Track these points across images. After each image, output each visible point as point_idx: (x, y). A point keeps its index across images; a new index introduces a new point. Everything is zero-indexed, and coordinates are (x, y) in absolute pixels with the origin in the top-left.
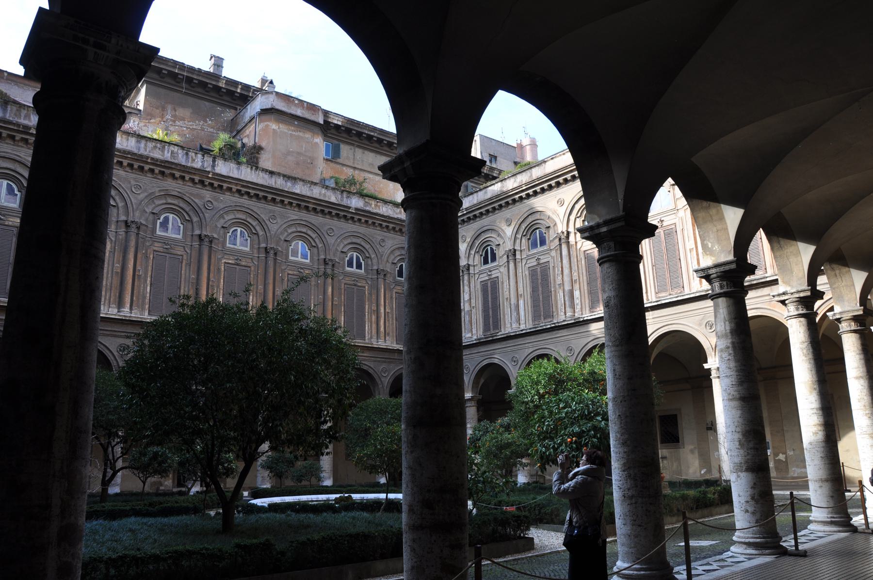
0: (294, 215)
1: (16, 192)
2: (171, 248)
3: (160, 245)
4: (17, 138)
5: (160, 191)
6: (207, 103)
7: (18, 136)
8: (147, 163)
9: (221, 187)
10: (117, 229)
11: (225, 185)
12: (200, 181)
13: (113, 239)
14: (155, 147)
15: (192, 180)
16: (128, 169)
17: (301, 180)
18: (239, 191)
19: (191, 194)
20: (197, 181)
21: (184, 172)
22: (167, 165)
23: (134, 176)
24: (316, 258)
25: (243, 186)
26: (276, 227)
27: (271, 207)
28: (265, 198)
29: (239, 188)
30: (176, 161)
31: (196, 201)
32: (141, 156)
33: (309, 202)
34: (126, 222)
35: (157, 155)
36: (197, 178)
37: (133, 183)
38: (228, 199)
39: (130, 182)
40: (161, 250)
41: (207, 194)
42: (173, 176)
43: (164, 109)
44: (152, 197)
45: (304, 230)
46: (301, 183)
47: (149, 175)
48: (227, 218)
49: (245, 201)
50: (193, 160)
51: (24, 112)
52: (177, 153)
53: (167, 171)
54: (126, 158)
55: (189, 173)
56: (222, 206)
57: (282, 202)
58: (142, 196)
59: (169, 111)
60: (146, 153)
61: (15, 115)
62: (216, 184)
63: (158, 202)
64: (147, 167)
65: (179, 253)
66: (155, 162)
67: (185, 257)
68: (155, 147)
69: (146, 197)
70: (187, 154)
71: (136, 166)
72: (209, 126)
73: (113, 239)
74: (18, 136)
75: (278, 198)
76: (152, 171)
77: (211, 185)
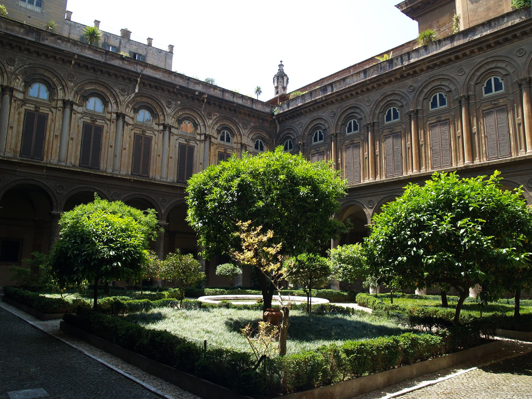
0: (479, 59)
2: (393, 130)
3: (387, 130)
5: (381, 96)
7: (315, 106)
8: (369, 84)
9: (415, 72)
11: (417, 69)
12: (400, 76)
15: (396, 79)
17: (478, 26)
18: (428, 68)
20: (399, 77)
23: (366, 95)
24: (509, 84)
25: (429, 62)
27: (457, 64)
28: (450, 60)
29: (427, 65)
31: (403, 90)
33: (488, 40)
38: (423, 78)
40: (388, 133)
41: (409, 82)
42: (385, 83)
45: (493, 65)
46: (481, 28)
48: (426, 91)
49: (437, 71)
54: (358, 88)
55: (392, 75)
57: (465, 55)
62: (411, 72)
63: (382, 104)
64: (369, 87)
65: (399, 130)
67: (402, 132)
75: (460, 54)
77: (409, 74)
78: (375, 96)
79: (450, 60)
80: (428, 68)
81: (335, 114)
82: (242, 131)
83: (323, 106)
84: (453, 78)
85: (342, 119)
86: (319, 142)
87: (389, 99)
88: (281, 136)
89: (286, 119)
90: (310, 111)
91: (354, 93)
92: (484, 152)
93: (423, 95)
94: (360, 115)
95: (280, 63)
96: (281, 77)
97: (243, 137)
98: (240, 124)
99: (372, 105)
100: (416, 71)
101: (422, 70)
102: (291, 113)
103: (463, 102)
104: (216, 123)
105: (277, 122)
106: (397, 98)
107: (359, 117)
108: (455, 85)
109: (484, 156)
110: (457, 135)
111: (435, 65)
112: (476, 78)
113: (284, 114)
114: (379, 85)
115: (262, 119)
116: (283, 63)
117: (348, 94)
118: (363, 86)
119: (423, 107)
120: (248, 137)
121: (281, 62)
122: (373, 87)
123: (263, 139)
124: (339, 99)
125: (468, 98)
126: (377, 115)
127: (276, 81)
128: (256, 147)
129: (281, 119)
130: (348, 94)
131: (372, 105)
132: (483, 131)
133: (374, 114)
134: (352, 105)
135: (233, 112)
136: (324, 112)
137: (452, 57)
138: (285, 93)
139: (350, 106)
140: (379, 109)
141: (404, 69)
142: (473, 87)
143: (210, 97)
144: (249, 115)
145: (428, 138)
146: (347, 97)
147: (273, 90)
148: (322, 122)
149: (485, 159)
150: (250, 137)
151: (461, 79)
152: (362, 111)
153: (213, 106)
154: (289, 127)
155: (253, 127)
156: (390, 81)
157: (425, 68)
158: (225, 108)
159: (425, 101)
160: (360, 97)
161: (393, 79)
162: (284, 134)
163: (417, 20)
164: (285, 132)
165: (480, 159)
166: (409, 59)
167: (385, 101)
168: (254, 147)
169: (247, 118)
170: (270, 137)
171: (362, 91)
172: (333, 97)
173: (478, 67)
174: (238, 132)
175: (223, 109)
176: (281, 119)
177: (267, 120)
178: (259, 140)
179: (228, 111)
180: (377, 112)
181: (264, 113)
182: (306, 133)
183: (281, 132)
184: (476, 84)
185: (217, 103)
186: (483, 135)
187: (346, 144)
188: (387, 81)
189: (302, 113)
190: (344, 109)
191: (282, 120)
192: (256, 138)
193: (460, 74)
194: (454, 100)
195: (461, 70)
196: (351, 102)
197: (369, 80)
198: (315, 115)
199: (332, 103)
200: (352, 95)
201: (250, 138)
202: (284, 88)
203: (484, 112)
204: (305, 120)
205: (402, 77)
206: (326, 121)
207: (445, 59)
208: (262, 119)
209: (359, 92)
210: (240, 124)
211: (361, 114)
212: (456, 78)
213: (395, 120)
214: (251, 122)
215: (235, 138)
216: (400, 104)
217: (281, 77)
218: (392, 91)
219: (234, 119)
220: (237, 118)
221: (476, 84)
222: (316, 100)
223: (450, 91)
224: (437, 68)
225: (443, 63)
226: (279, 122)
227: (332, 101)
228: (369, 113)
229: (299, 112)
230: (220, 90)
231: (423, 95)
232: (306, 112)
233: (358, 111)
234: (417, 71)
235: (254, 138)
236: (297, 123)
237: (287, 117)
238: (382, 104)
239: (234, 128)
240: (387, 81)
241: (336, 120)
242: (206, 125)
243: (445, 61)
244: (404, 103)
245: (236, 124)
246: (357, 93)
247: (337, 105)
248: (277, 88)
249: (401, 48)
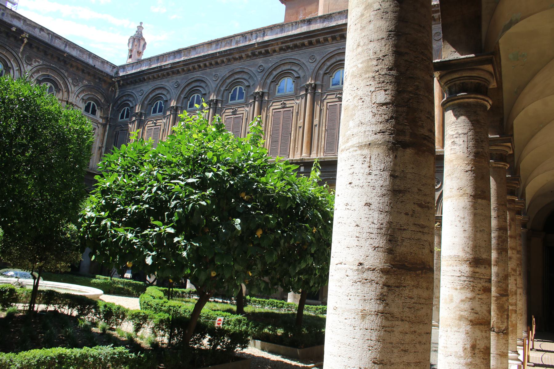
5: (229, 72)
7: (160, 74)
8: (218, 57)
9: (267, 52)
11: (269, 49)
12: (252, 53)
15: (248, 56)
18: (281, 49)
20: (250, 54)
25: (282, 43)
26: (314, 65)
28: (303, 45)
29: (280, 46)
31: (252, 69)
36: (249, 53)
38: (274, 59)
41: (260, 61)
42: (235, 59)
46: (338, 16)
48: (275, 73)
49: (289, 54)
54: (206, 60)
55: (243, 51)
56: (270, 65)
57: (318, 42)
62: (263, 51)
63: (228, 81)
64: (219, 60)
75: (314, 40)
77: (260, 53)
78: (224, 71)
79: (303, 45)
80: (281, 49)
81: (179, 85)
82: (72, 88)
83: (168, 74)
84: (304, 63)
85: (186, 92)
86: (157, 114)
87: (236, 76)
88: (119, 102)
89: (128, 84)
90: (154, 78)
91: (202, 65)
92: (322, 146)
93: (272, 77)
95: (139, 25)
96: (138, 40)
97: (70, 95)
98: (70, 79)
99: (219, 80)
100: (268, 50)
101: (274, 51)
102: (132, 78)
103: (309, 91)
104: (37, 71)
106: (245, 76)
107: (203, 92)
108: (304, 71)
109: (322, 151)
110: (298, 125)
111: (288, 48)
112: (326, 67)
113: (126, 77)
114: (229, 60)
115: (100, 79)
116: (142, 25)
118: (212, 58)
119: (269, 90)
120: (78, 96)
121: (141, 23)
122: (223, 62)
123: (96, 101)
124: (185, 69)
125: (315, 88)
126: (222, 92)
127: (131, 42)
128: (87, 109)
130: (196, 65)
131: (219, 80)
132: (324, 125)
133: (219, 90)
134: (198, 78)
135: (62, 63)
136: (168, 81)
137: (306, 42)
138: (139, 58)
140: (225, 86)
141: (256, 46)
142: (321, 76)
143: (32, 38)
144: (83, 71)
145: (270, 124)
146: (194, 68)
147: (126, 54)
148: (165, 92)
149: (322, 154)
150: (81, 96)
151: (311, 67)
152: (207, 85)
153: (35, 50)
154: (129, 93)
155: (86, 86)
156: (241, 58)
157: (277, 49)
158: (52, 56)
159: (273, 84)
160: (208, 70)
161: (243, 55)
162: (122, 100)
163: (285, 4)
164: (124, 98)
165: (317, 154)
166: (264, 36)
167: (233, 79)
168: (83, 109)
169: (80, 73)
170: (107, 101)
171: (211, 64)
172: (179, 66)
173: (329, 56)
174: (65, 87)
175: (49, 57)
176: (122, 82)
177: (105, 81)
178: (92, 102)
179: (56, 60)
180: (222, 89)
181: (102, 72)
182: (146, 103)
183: (119, 98)
184: (325, 74)
185: (41, 48)
186: (324, 129)
188: (237, 56)
189: (145, 80)
191: (123, 84)
192: (88, 99)
193: (310, 61)
194: (301, 88)
195: (312, 57)
196: (198, 75)
197: (219, 52)
198: (158, 83)
199: (178, 72)
200: (199, 66)
201: (81, 97)
202: (140, 53)
203: (329, 104)
204: (147, 88)
205: (254, 54)
206: (168, 92)
207: (298, 42)
208: (100, 79)
209: (208, 64)
210: (70, 79)
211: (206, 89)
212: (306, 64)
213: (240, 101)
214: (84, 79)
215: (61, 93)
216: (247, 84)
217: (138, 40)
218: (241, 68)
219: (63, 71)
220: (67, 71)
221: (325, 74)
222: (161, 67)
223: (299, 77)
224: (290, 50)
225: (296, 46)
226: (119, 86)
227: (178, 70)
228: (214, 89)
229: (141, 78)
230: (49, 34)
231: (272, 77)
232: (149, 79)
233: (203, 85)
234: (270, 50)
235: (85, 98)
236: (139, 89)
238: (228, 81)
239: (61, 82)
240: (237, 56)
241: (179, 92)
242: (23, 70)
243: (298, 44)
244: (252, 84)
245: (63, 78)
247: (183, 76)
248: (131, 51)
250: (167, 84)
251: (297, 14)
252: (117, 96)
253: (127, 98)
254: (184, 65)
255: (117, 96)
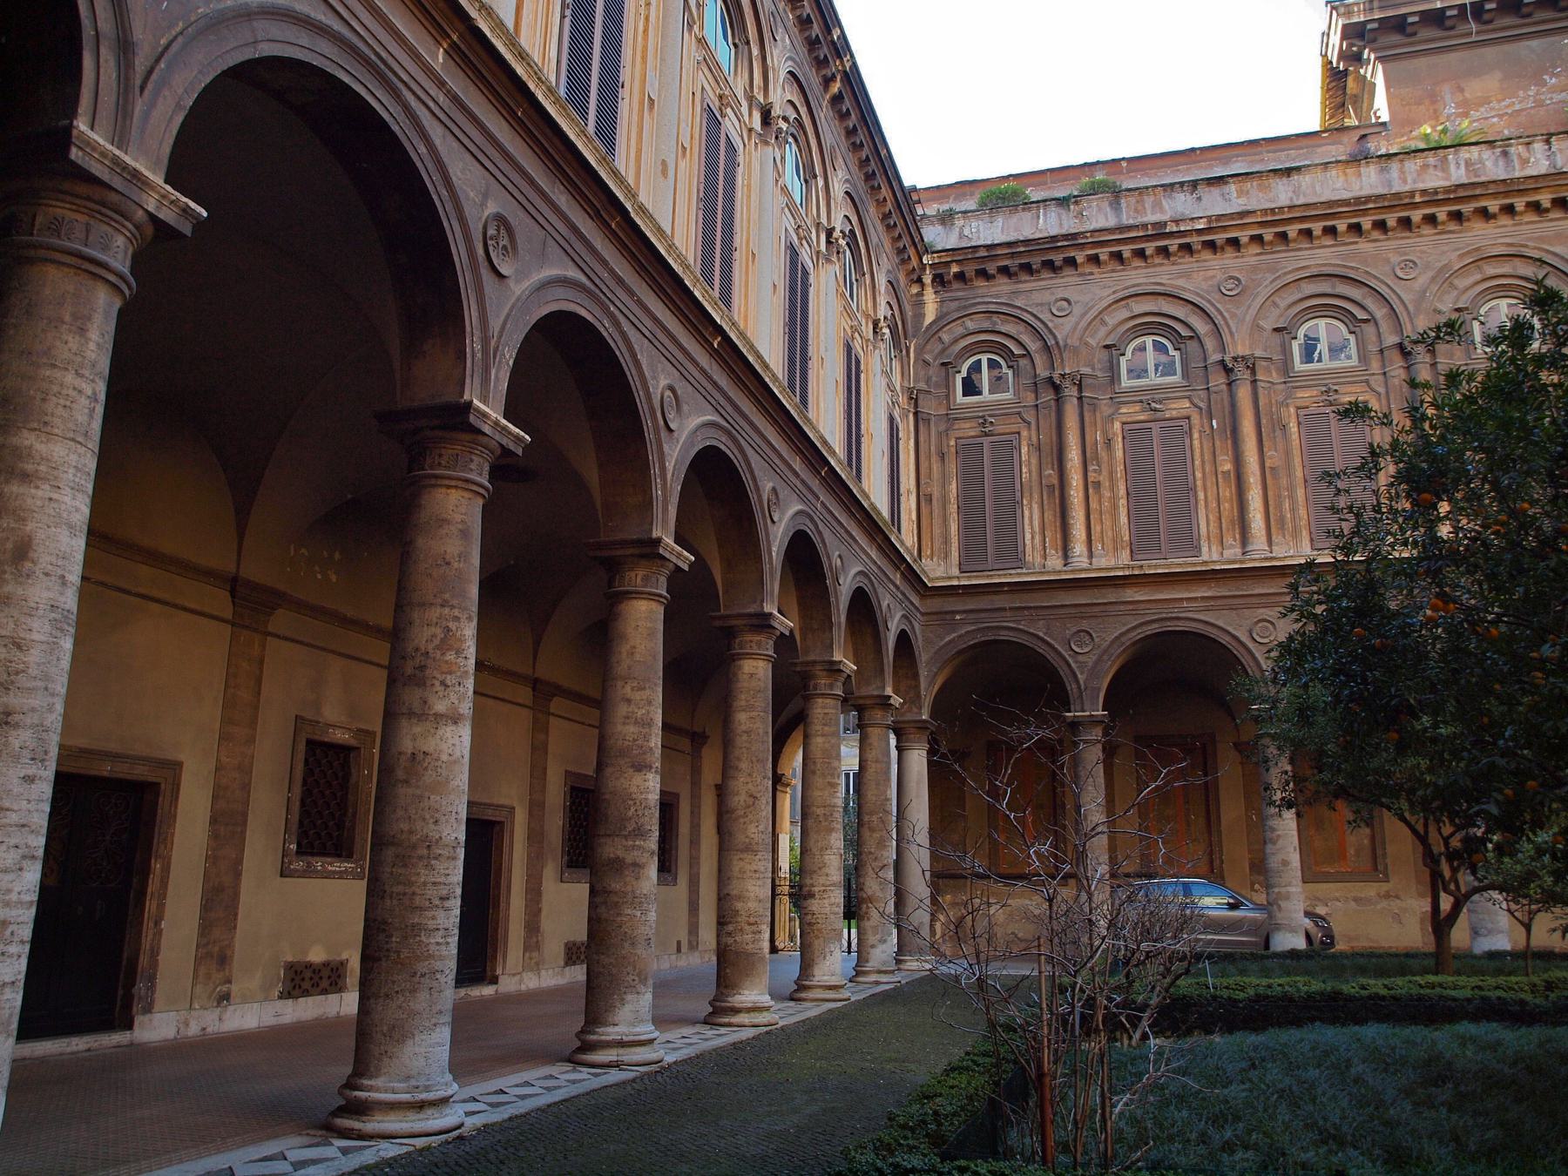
1: (1172, 352)
4: (1148, 252)
5: (1461, 256)
6: (1534, 43)
7: (1150, 248)
8: (1415, 206)
10: (1384, 366)
13: (1382, 390)
14: (1425, 166)
15: (1535, 207)
16: (1376, 234)
19: (1541, 239)
21: (1507, 194)
22: (1461, 193)
23: (1393, 244)
30: (1483, 179)
31: (1557, 249)
32: (1397, 195)
34: (1401, 346)
35: (1434, 181)
37: (1395, 259)
39: (1388, 260)
42: (1484, 214)
43: (1434, 98)
44: (1445, 277)
47: (1427, 230)
50: (1525, 162)
51: (1149, 200)
52: (1481, 161)
53: (1467, 208)
54: (1365, 212)
58: (1422, 280)
59: (1448, 97)
60: (1407, 188)
61: (1136, 211)
63: (1462, 283)
64: (1416, 216)
66: (1433, 198)
68: (1425, 166)
69: (1433, 279)
70: (1505, 154)
71: (1391, 223)
72: (1553, 90)
73: (1382, 390)
74: (1150, 248)
76: (1431, 220)
87: (1491, 270)
89: (983, 274)
90: (1118, 256)
91: (1341, 226)
94: (1363, 307)
105: (927, 279)
113: (983, 253)
117: (1317, 228)
129: (955, 269)
136: (1187, 275)
139: (1315, 271)
154: (992, 308)
160: (1363, 246)
187: (1300, 403)
190: (1290, 278)
191: (960, 276)
200: (1331, 231)
209: (1366, 222)
229: (1058, 258)
236: (1037, 297)
237: (991, 268)
241: (1253, 311)
246: (1356, 229)
249: (1305, 142)
250: (1181, 282)
251: (1434, 102)
252: (930, 317)
253: (986, 325)
254: (1262, 224)
255: (930, 317)
